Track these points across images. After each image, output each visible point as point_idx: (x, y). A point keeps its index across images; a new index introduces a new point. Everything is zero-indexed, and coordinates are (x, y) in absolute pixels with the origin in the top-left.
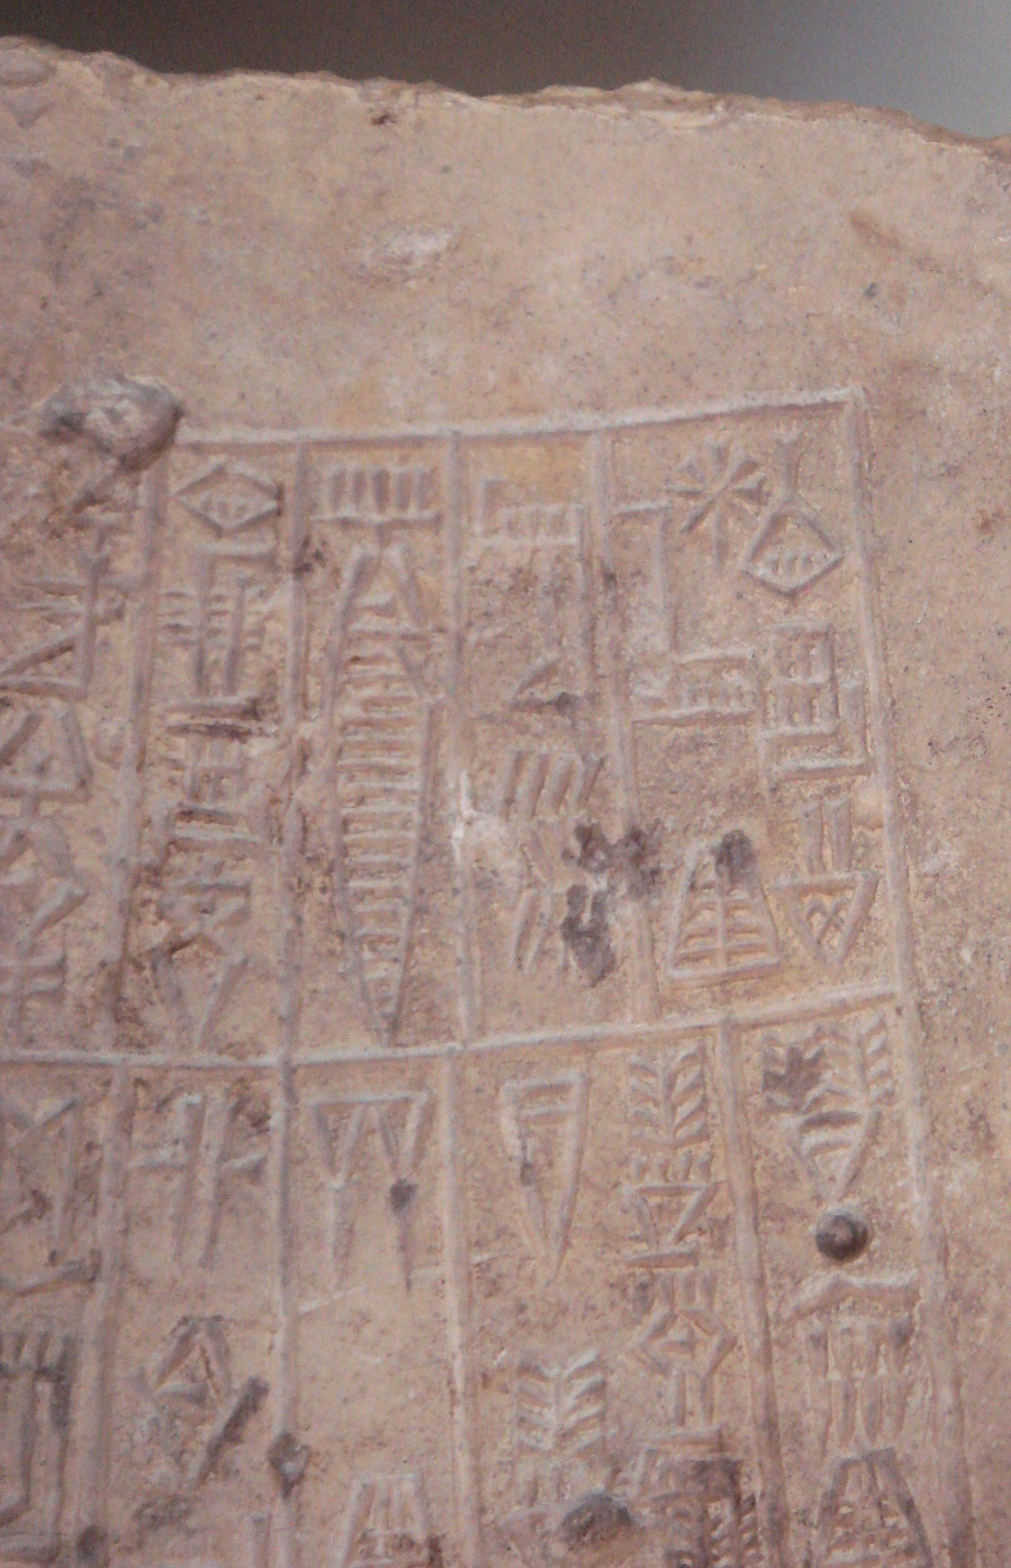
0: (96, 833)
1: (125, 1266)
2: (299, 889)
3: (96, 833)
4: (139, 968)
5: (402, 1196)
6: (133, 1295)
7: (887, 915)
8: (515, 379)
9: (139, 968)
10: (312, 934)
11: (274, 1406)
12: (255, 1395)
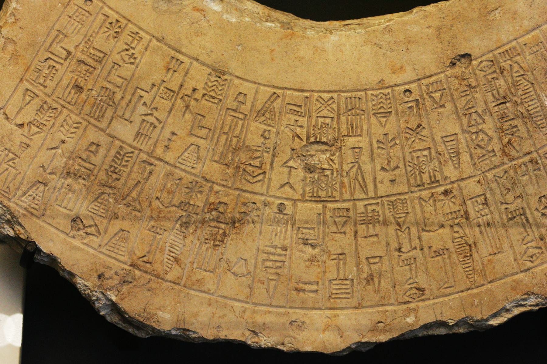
0: (490, 128)
1: (526, 193)
2: (525, 123)
3: (490, 128)
4: (506, 147)
6: (530, 197)
8: (521, 26)
9: (506, 147)
10: (531, 129)
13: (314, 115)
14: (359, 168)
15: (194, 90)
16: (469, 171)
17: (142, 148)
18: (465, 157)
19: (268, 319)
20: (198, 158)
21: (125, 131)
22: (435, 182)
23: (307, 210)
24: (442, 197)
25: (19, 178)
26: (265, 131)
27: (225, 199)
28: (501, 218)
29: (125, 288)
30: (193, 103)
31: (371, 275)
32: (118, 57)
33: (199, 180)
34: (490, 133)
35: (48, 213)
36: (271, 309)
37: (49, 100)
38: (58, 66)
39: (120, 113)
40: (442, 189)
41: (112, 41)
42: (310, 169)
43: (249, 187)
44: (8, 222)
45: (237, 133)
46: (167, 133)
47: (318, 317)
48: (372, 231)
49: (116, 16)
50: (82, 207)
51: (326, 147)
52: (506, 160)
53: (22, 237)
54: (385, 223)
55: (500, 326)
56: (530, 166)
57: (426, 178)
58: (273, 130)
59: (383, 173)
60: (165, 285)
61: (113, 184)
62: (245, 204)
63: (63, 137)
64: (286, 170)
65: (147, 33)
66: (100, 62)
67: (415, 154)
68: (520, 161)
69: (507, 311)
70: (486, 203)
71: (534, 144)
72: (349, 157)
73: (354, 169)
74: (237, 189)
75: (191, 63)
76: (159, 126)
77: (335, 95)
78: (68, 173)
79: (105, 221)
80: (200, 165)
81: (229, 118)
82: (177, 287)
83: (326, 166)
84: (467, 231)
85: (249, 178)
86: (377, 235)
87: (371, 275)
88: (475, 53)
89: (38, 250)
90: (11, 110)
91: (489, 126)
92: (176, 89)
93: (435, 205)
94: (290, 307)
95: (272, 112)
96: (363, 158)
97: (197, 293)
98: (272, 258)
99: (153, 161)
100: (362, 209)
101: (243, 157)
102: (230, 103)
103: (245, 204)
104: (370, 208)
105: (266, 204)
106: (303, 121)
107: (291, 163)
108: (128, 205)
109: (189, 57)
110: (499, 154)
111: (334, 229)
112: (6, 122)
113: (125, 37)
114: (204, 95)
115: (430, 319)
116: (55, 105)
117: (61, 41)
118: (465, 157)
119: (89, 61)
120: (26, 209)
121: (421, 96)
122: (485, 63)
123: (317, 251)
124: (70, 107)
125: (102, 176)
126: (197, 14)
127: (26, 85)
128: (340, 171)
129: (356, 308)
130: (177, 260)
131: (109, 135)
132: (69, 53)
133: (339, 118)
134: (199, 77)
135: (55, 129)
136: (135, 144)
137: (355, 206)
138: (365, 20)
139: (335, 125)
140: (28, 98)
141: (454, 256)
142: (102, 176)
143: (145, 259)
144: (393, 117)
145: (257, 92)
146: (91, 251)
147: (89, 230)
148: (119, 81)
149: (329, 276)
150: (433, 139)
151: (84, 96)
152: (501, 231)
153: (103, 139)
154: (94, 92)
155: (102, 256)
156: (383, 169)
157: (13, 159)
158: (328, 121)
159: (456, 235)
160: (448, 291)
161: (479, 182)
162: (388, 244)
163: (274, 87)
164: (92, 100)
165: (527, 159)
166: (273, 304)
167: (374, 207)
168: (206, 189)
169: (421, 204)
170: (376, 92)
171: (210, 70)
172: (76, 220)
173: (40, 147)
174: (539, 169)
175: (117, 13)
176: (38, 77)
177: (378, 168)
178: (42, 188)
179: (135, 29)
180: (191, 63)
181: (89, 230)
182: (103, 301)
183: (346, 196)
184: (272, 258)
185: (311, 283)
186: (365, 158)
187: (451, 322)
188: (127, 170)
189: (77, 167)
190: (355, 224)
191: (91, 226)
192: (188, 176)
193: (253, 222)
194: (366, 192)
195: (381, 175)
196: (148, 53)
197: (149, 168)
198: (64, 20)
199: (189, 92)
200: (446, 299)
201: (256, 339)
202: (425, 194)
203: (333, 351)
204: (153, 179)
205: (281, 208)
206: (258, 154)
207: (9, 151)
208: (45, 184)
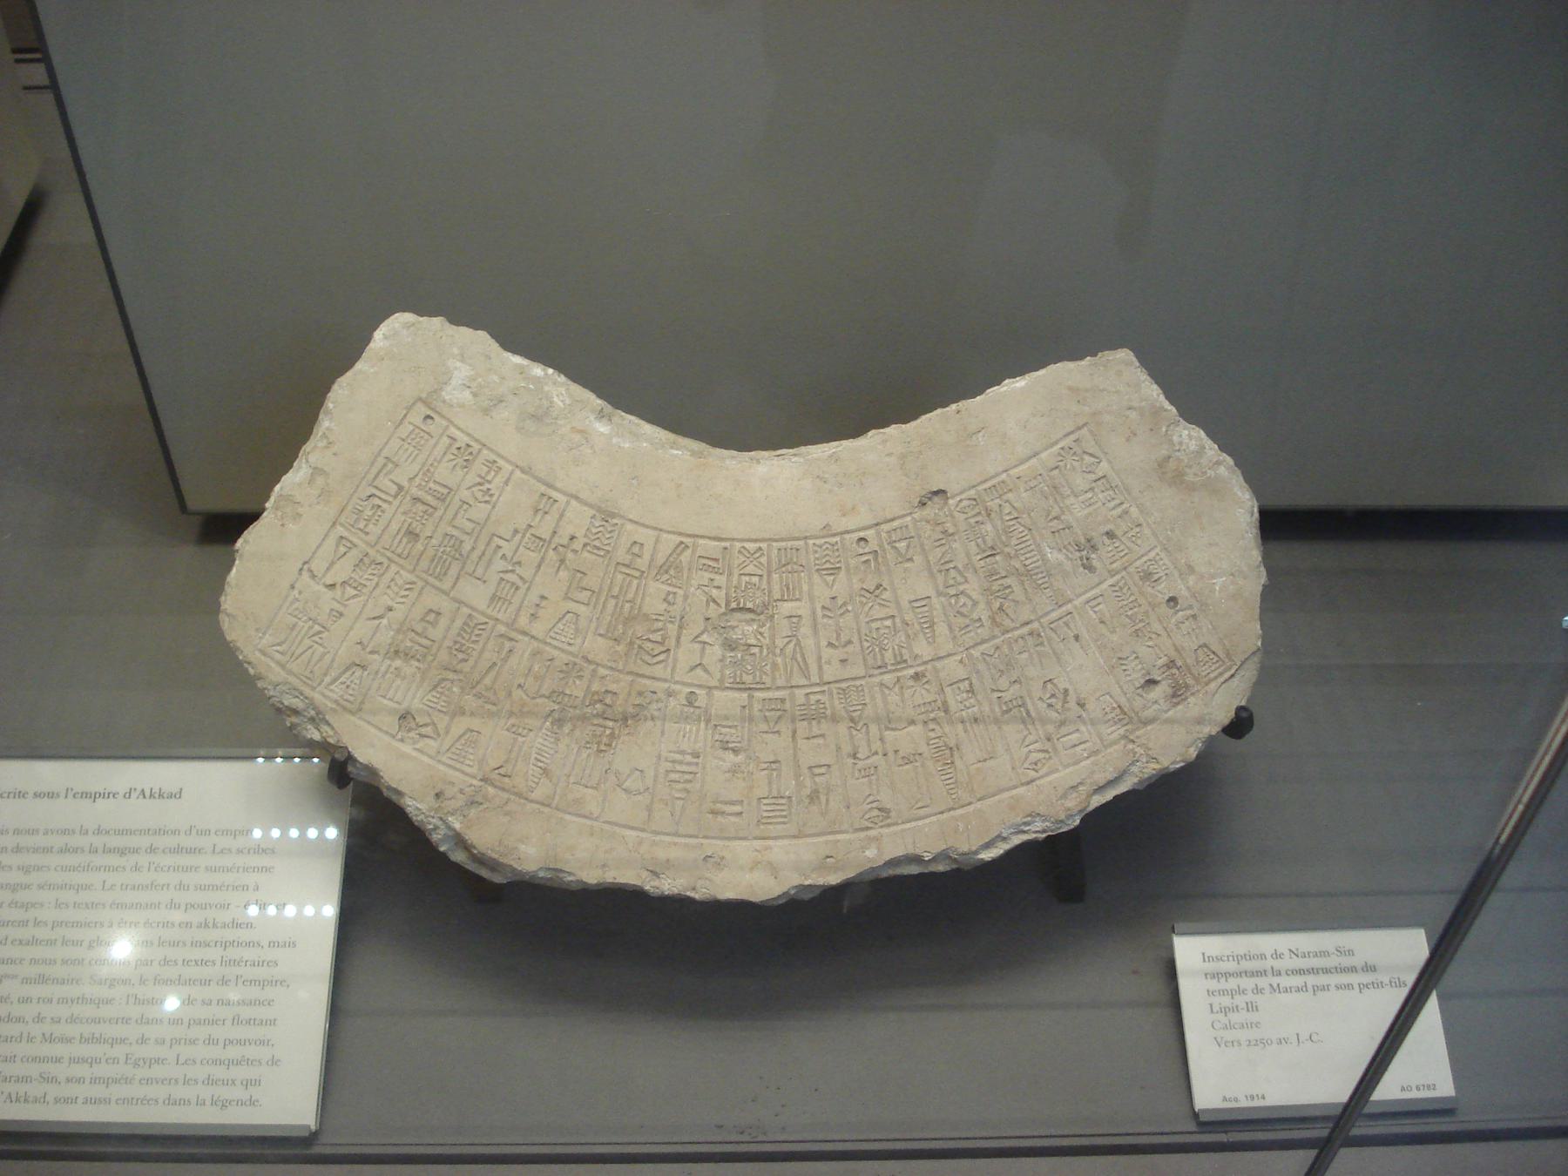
2: (1022, 583)
5: (1077, 638)
7: (1147, 531)
11: (1071, 692)
12: (1066, 691)
13: (736, 572)
14: (798, 643)
15: (572, 538)
16: (949, 647)
17: (500, 616)
18: (942, 629)
19: (674, 854)
20: (577, 630)
21: (476, 594)
22: (901, 662)
23: (727, 701)
24: (911, 683)
25: (328, 658)
26: (669, 593)
27: (613, 687)
28: (992, 711)
29: (473, 812)
30: (570, 555)
31: (816, 791)
32: (466, 493)
33: (578, 661)
34: (974, 595)
35: (366, 706)
36: (676, 840)
37: (372, 552)
38: (385, 506)
39: (470, 568)
40: (911, 671)
41: (460, 473)
42: (730, 645)
43: (647, 670)
44: (312, 720)
45: (630, 596)
46: (533, 597)
47: (742, 850)
48: (816, 731)
49: (466, 439)
50: (416, 700)
51: (751, 616)
52: (997, 631)
53: (331, 741)
54: (835, 719)
55: (994, 861)
56: (1030, 641)
57: (889, 656)
58: (681, 592)
59: (831, 651)
60: (530, 806)
61: (459, 667)
62: (640, 694)
63: (390, 603)
64: (697, 646)
65: (508, 461)
66: (443, 500)
67: (874, 625)
68: (1017, 633)
69: (1004, 839)
70: (971, 691)
71: (1034, 611)
72: (784, 628)
73: (791, 645)
74: (631, 673)
75: (568, 503)
76: (524, 587)
77: (764, 545)
78: (397, 652)
79: (447, 718)
80: (579, 641)
81: (620, 577)
82: (546, 810)
83: (753, 641)
84: (947, 729)
85: (647, 658)
86: (822, 736)
87: (816, 791)
88: (952, 488)
89: (350, 758)
90: (318, 565)
91: (973, 587)
92: (546, 536)
93: (902, 694)
94: (705, 837)
95: (679, 569)
96: (803, 630)
97: (574, 819)
98: (678, 768)
99: (513, 634)
100: (802, 700)
101: (640, 629)
102: (621, 555)
103: (640, 694)
104: (813, 698)
105: (670, 694)
106: (721, 580)
107: (704, 637)
108: (479, 696)
109: (564, 493)
110: (987, 623)
111: (764, 727)
112: (312, 583)
113: (479, 467)
114: (585, 545)
115: (900, 852)
116: (380, 559)
117: (390, 472)
118: (942, 629)
119: (429, 499)
120: (336, 702)
121: (881, 546)
122: (965, 503)
123: (741, 758)
124: (401, 561)
125: (443, 656)
126: (577, 438)
127: (340, 530)
128: (771, 651)
129: (795, 837)
130: (546, 772)
131: (455, 600)
132: (401, 488)
133: (769, 575)
134: (578, 520)
135: (377, 592)
136: (489, 611)
137: (792, 696)
138: (803, 449)
139: (764, 585)
140: (342, 549)
141: (930, 764)
142: (443, 656)
143: (502, 771)
144: (842, 574)
145: (657, 541)
146: (425, 759)
147: (423, 730)
148: (469, 526)
149: (759, 793)
150: (898, 603)
151: (420, 547)
152: (993, 728)
153: (446, 605)
154: (434, 541)
155: (442, 768)
156: (830, 644)
157: (320, 632)
158: (755, 579)
159: (932, 735)
160: (922, 812)
161: (961, 661)
162: (839, 749)
163: (680, 534)
164: (430, 552)
165: (1025, 630)
166: (682, 830)
167: (818, 697)
168: (587, 674)
169: (883, 693)
170: (818, 542)
171: (593, 512)
172: (404, 716)
173: (357, 618)
174: (1042, 644)
175: (469, 435)
176: (357, 521)
177: (824, 643)
178: (359, 672)
179: (493, 457)
180: (568, 503)
181: (423, 730)
182: (443, 831)
183: (780, 682)
184: (678, 768)
185: (732, 803)
186: (805, 630)
187: (927, 857)
188: (478, 647)
189: (409, 644)
190: (793, 721)
191: (426, 725)
192: (563, 656)
193: (653, 719)
194: (808, 677)
195: (827, 653)
196: (508, 488)
197: (508, 645)
198: (395, 443)
199: (565, 541)
200: (920, 823)
201: (656, 883)
202: (888, 678)
203: (764, 898)
204: (513, 661)
205: (691, 700)
206: (660, 624)
207: (315, 621)
208: (364, 668)
